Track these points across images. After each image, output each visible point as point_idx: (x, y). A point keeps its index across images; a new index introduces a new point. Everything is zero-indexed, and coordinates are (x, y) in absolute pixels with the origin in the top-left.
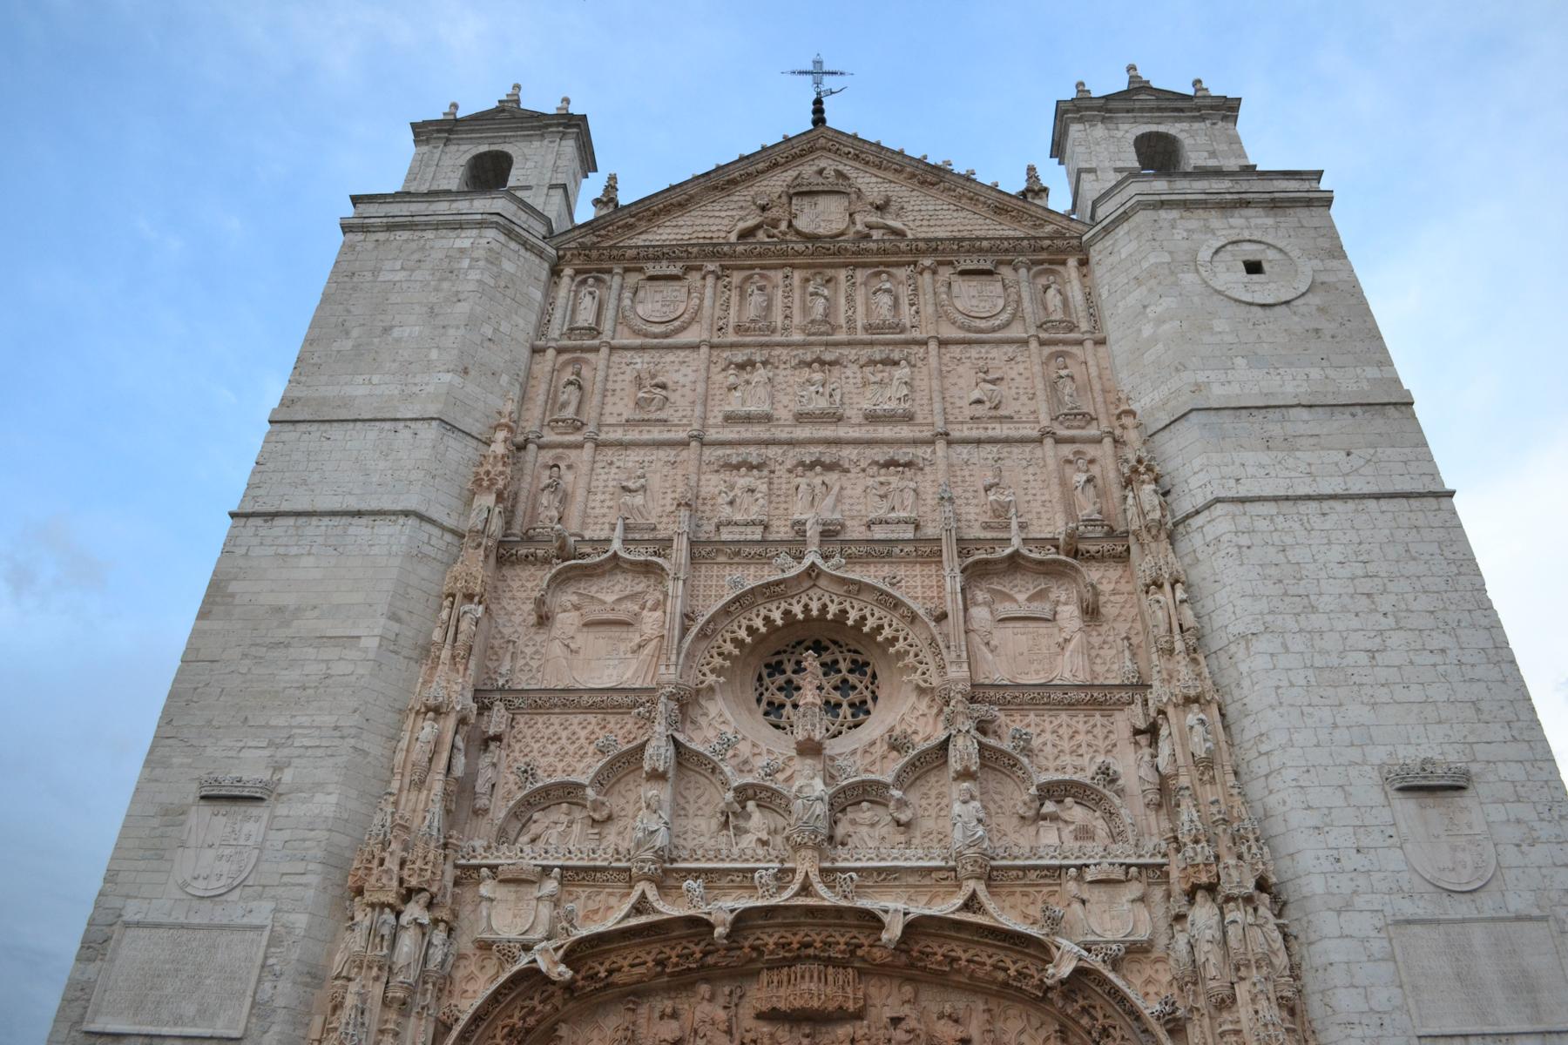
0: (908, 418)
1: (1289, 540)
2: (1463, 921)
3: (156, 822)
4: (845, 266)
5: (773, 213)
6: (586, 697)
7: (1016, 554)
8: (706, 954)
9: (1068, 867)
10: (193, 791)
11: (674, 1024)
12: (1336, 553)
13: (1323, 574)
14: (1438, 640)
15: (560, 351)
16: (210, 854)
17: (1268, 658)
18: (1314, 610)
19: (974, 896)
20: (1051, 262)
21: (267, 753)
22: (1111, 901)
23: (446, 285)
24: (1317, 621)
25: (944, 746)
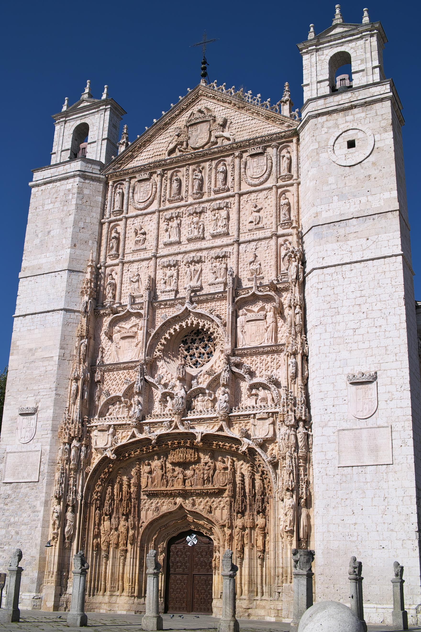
0: (227, 234)
1: (336, 284)
2: (361, 429)
3: (10, 422)
5: (181, 139)
7: (254, 294)
8: (153, 448)
9: (251, 414)
10: (17, 412)
11: (149, 467)
13: (345, 298)
14: (381, 322)
15: (110, 223)
16: (24, 431)
17: (319, 335)
18: (338, 313)
19: (222, 426)
20: (287, 142)
21: (34, 398)
22: (263, 424)
23: (65, 208)
24: (339, 318)
25: (220, 374)
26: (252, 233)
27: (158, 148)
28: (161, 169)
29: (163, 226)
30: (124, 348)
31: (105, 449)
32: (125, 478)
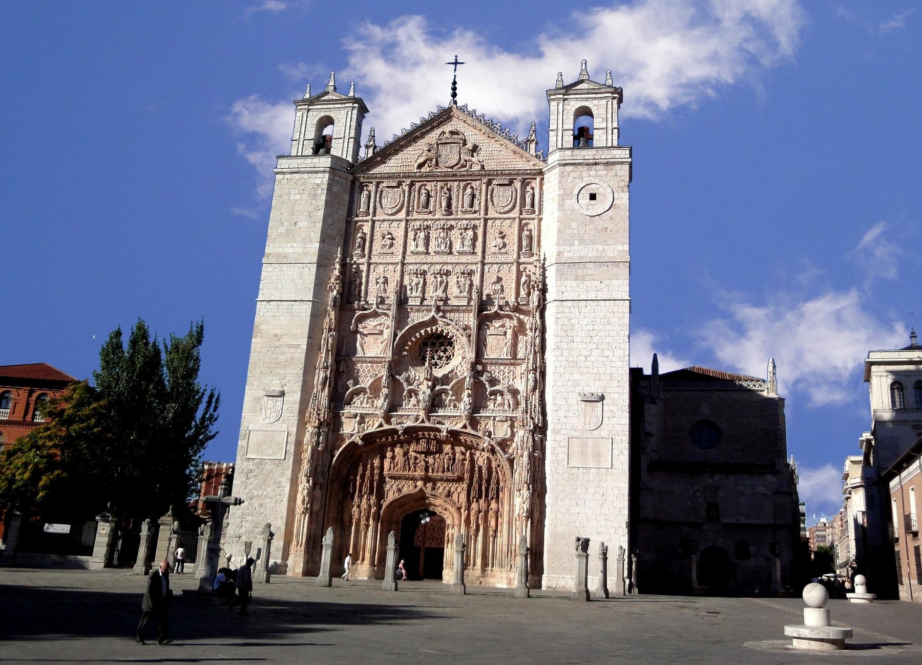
7: (496, 312)
12: (586, 321)
23: (314, 202)
24: (574, 345)
29: (411, 235)
30: (375, 345)
31: (352, 435)
32: (376, 462)
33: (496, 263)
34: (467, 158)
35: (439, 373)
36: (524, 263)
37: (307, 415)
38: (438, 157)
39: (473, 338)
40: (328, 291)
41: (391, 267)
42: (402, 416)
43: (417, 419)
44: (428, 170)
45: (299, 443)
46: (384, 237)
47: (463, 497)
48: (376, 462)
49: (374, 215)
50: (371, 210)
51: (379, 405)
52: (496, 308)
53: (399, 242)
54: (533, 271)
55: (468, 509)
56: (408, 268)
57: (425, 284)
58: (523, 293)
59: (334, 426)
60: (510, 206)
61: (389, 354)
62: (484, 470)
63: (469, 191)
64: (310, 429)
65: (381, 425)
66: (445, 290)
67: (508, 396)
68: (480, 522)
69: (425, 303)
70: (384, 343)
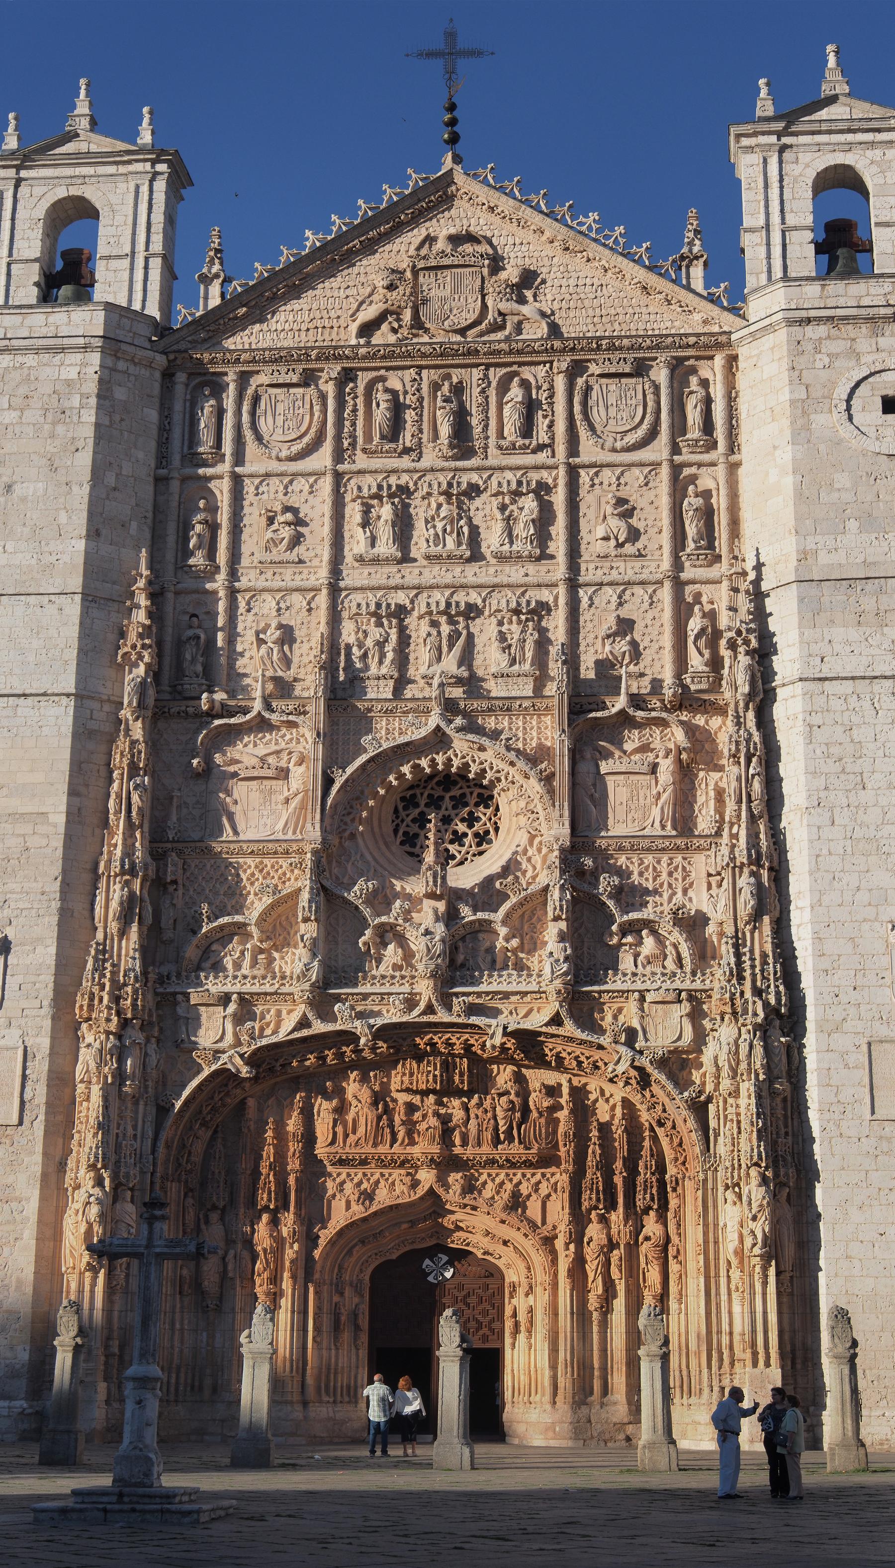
4: (477, 365)
6: (245, 846)
26: (608, 565)
27: (332, 311)
28: (339, 368)
29: (353, 512)
33: (610, 584)
34: (504, 306)
35: (466, 877)
36: (693, 582)
37: (81, 1001)
38: (418, 303)
39: (562, 783)
40: (120, 667)
41: (297, 600)
42: (365, 996)
43: (410, 1002)
44: (392, 339)
45: (61, 1083)
46: (271, 521)
47: (559, 1213)
48: (293, 1124)
49: (239, 458)
50: (228, 447)
51: (298, 968)
52: (620, 703)
53: (319, 531)
54: (720, 598)
55: (578, 1238)
56: (351, 602)
57: (404, 640)
58: (696, 661)
59: (161, 1030)
60: (641, 433)
61: (313, 833)
62: (618, 1131)
63: (516, 393)
64: (92, 1039)
65: (304, 1023)
66: (467, 658)
67: (676, 936)
68: (615, 1273)
69: (408, 693)
70: (294, 804)
